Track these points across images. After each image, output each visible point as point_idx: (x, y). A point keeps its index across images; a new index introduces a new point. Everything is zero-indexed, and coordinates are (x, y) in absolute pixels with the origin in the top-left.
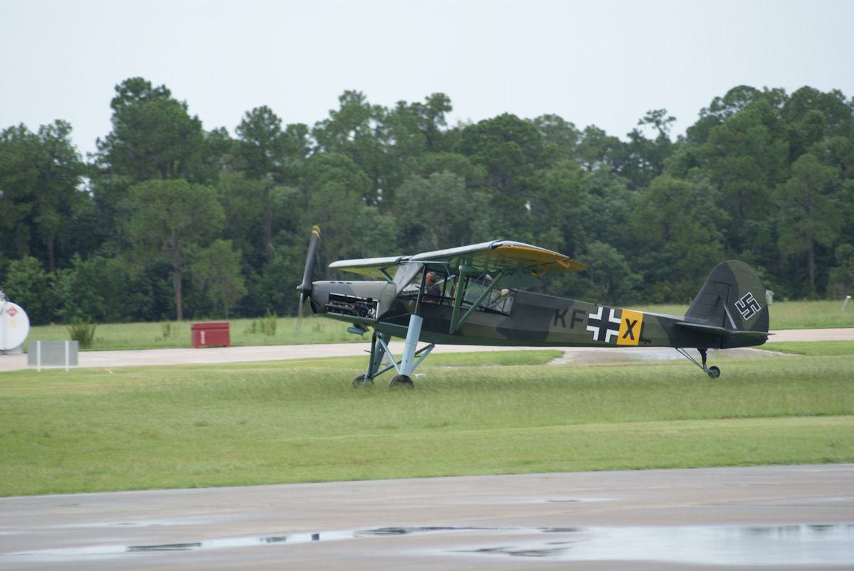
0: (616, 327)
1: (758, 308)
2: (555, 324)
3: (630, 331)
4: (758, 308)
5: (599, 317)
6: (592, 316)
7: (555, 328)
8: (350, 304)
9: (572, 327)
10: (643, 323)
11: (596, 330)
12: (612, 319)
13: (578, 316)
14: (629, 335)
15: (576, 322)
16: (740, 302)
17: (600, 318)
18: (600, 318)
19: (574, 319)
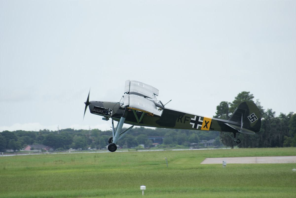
0: (201, 123)
1: (257, 119)
2: (178, 121)
3: (206, 125)
4: (257, 119)
5: (195, 119)
6: (192, 119)
8: (102, 110)
9: (184, 123)
10: (211, 123)
11: (193, 124)
12: (200, 120)
13: (187, 119)
14: (206, 127)
15: (186, 121)
16: (250, 116)
17: (195, 120)
18: (195, 120)
19: (185, 120)
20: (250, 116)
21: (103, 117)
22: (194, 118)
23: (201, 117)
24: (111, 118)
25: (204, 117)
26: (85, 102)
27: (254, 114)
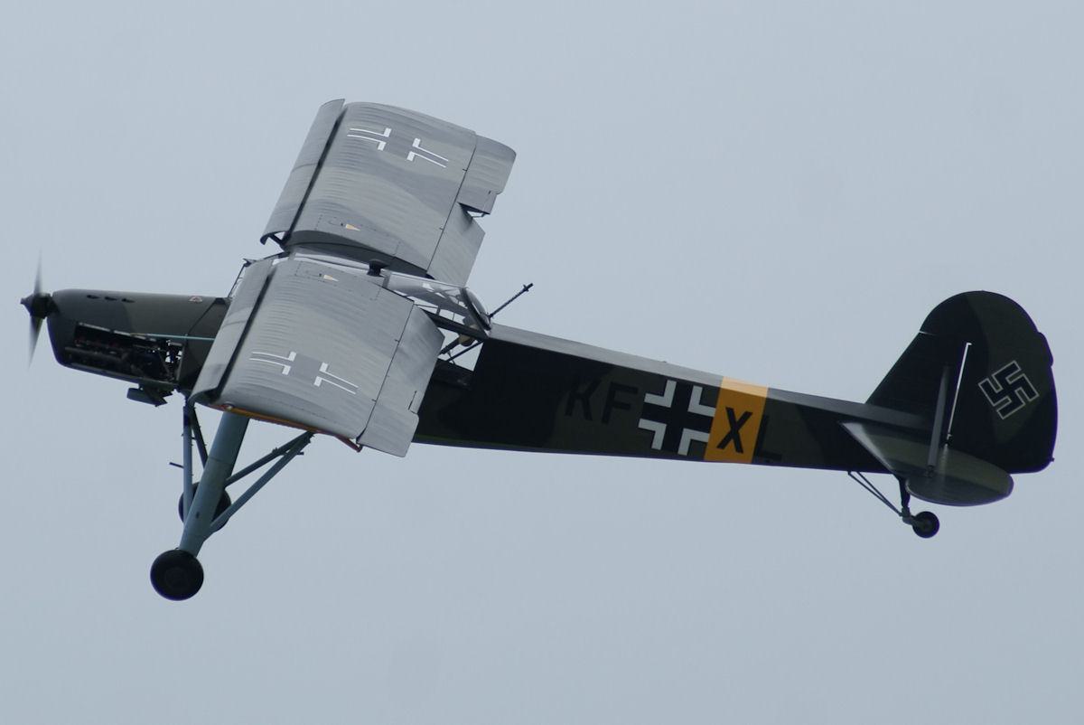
0: (703, 423)
1: (1031, 394)
4: (1031, 394)
5: (666, 400)
6: (651, 399)
10: (765, 420)
11: (659, 429)
12: (695, 406)
16: (992, 380)
20: (993, 376)
21: (136, 386)
22: (662, 394)
23: (701, 389)
24: (175, 392)
25: (724, 386)
26: (26, 296)
27: (1013, 367)
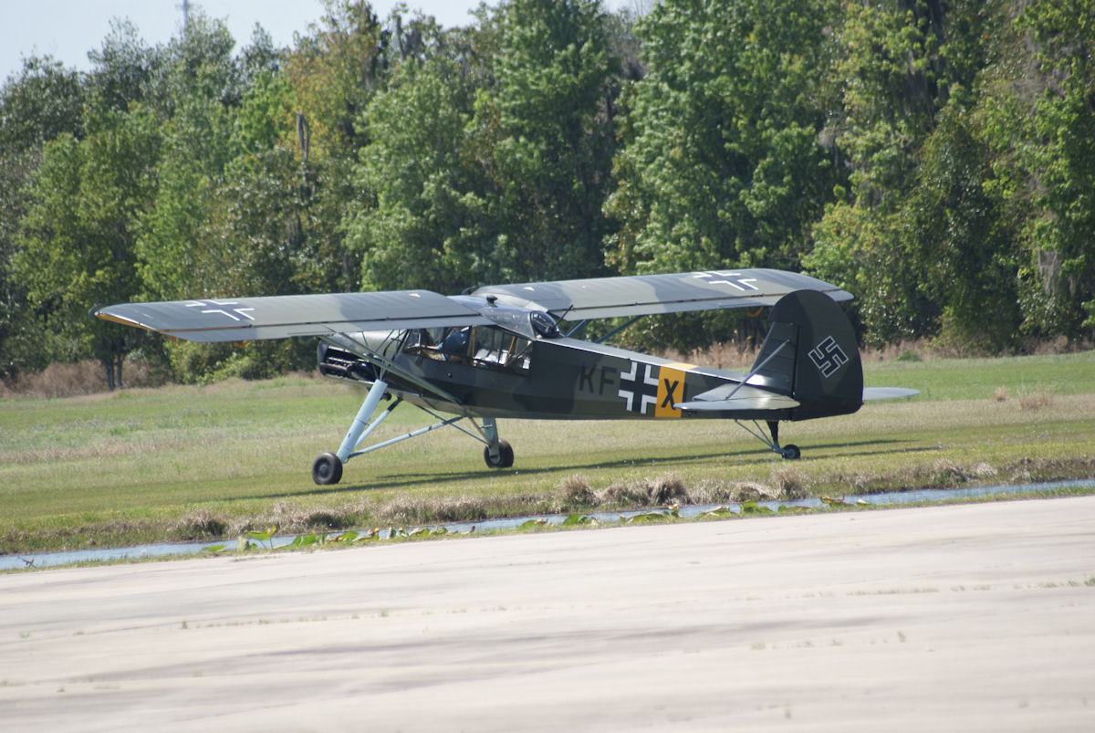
0: (652, 390)
1: (843, 359)
2: (581, 388)
4: (843, 359)
5: (631, 376)
6: (624, 376)
7: (582, 395)
9: (601, 392)
10: (686, 385)
11: (629, 396)
12: (648, 380)
13: (608, 376)
15: (605, 385)
16: (817, 350)
17: (633, 379)
18: (633, 379)
19: (604, 381)
27: (830, 341)
